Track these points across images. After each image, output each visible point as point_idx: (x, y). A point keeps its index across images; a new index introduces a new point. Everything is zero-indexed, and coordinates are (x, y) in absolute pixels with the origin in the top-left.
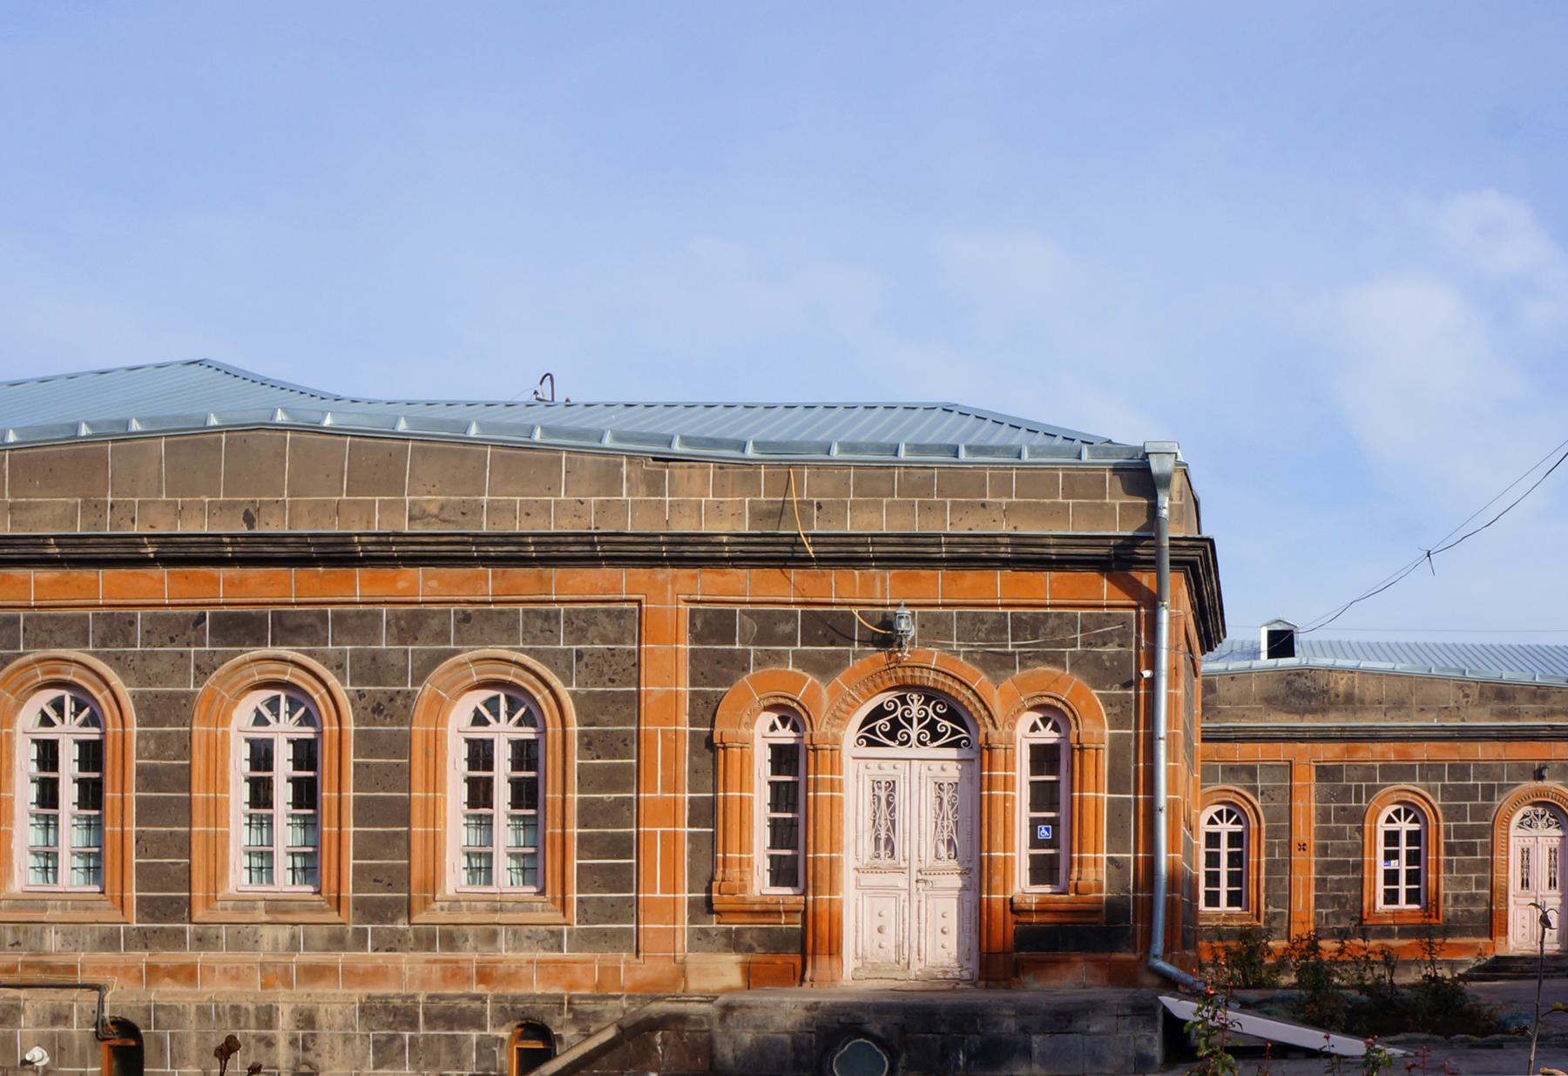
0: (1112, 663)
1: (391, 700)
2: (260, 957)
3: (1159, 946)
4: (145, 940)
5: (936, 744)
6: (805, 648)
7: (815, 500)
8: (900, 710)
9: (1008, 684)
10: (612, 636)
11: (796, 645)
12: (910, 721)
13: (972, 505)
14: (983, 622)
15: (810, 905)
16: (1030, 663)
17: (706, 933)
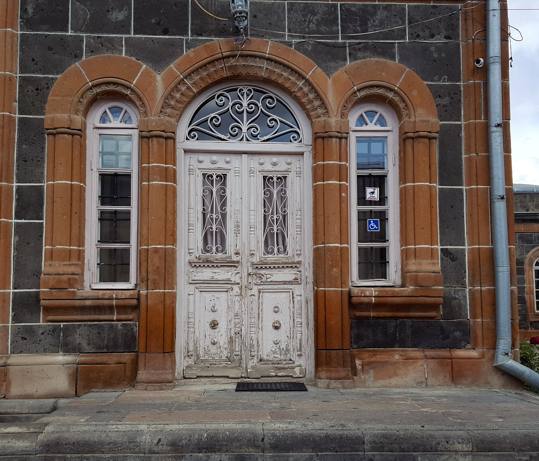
6: (137, 36)
8: (231, 104)
9: (340, 73)
11: (129, 33)
14: (314, 13)
15: (143, 300)
16: (360, 54)
17: (30, 330)
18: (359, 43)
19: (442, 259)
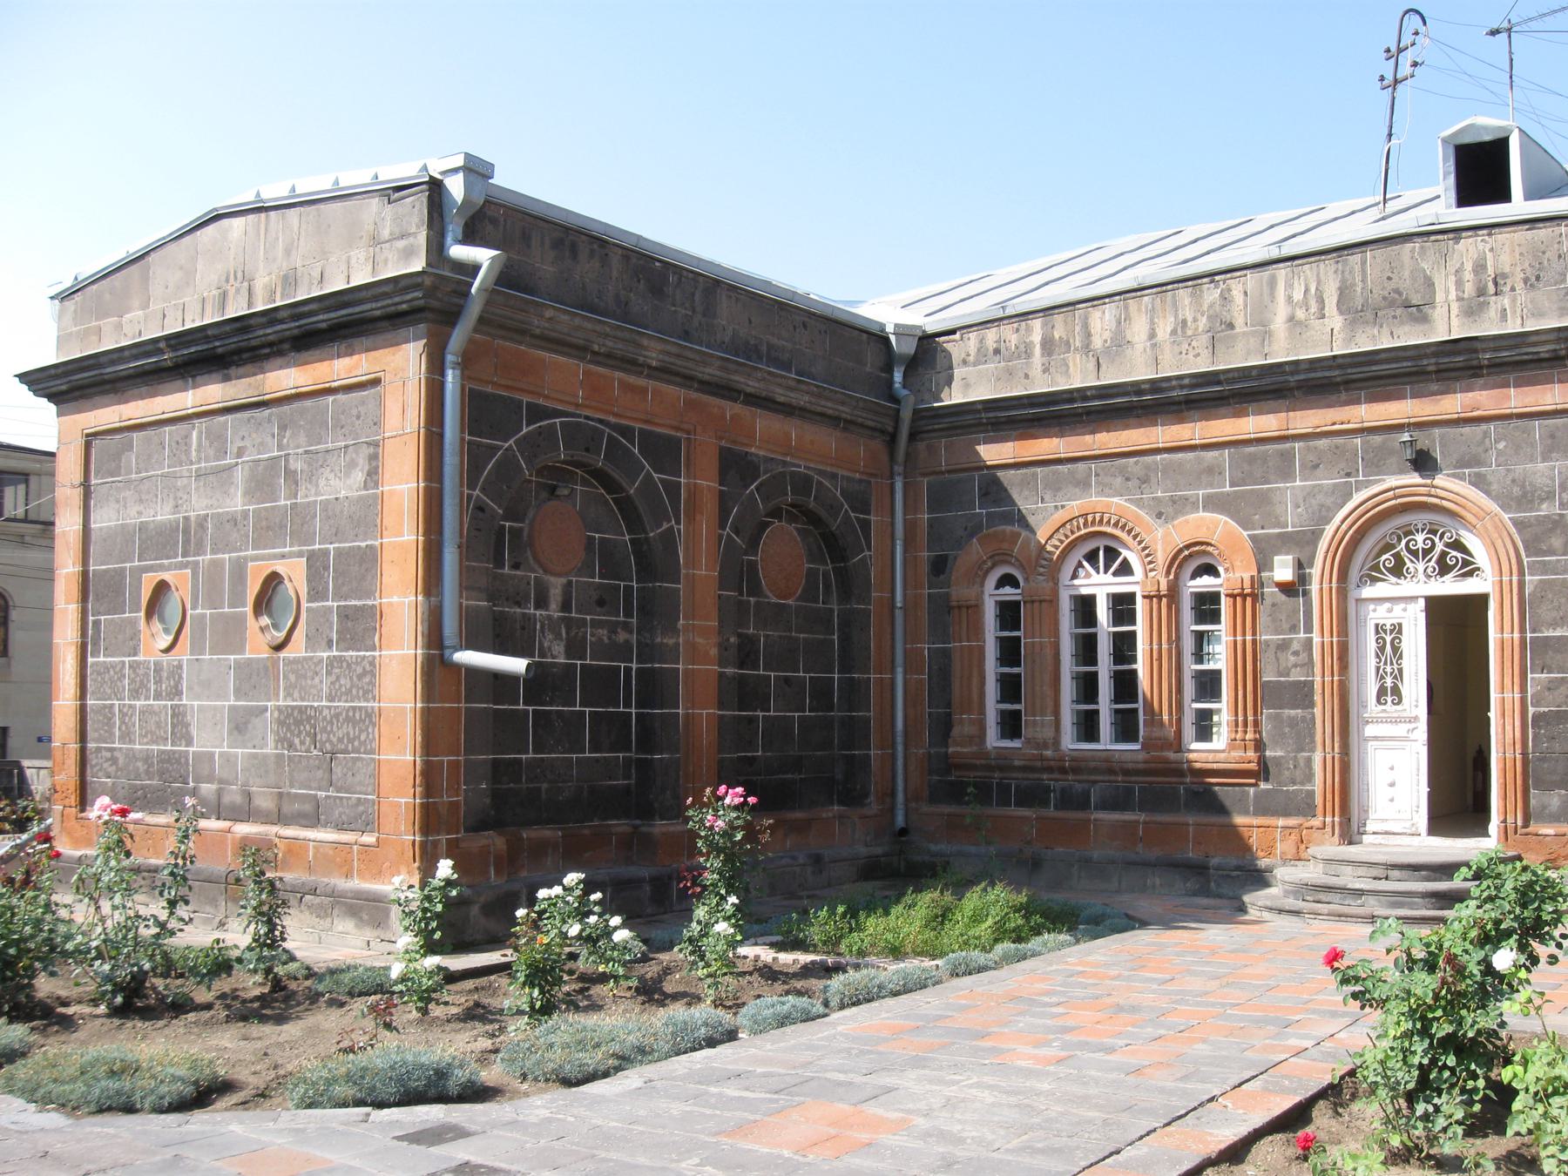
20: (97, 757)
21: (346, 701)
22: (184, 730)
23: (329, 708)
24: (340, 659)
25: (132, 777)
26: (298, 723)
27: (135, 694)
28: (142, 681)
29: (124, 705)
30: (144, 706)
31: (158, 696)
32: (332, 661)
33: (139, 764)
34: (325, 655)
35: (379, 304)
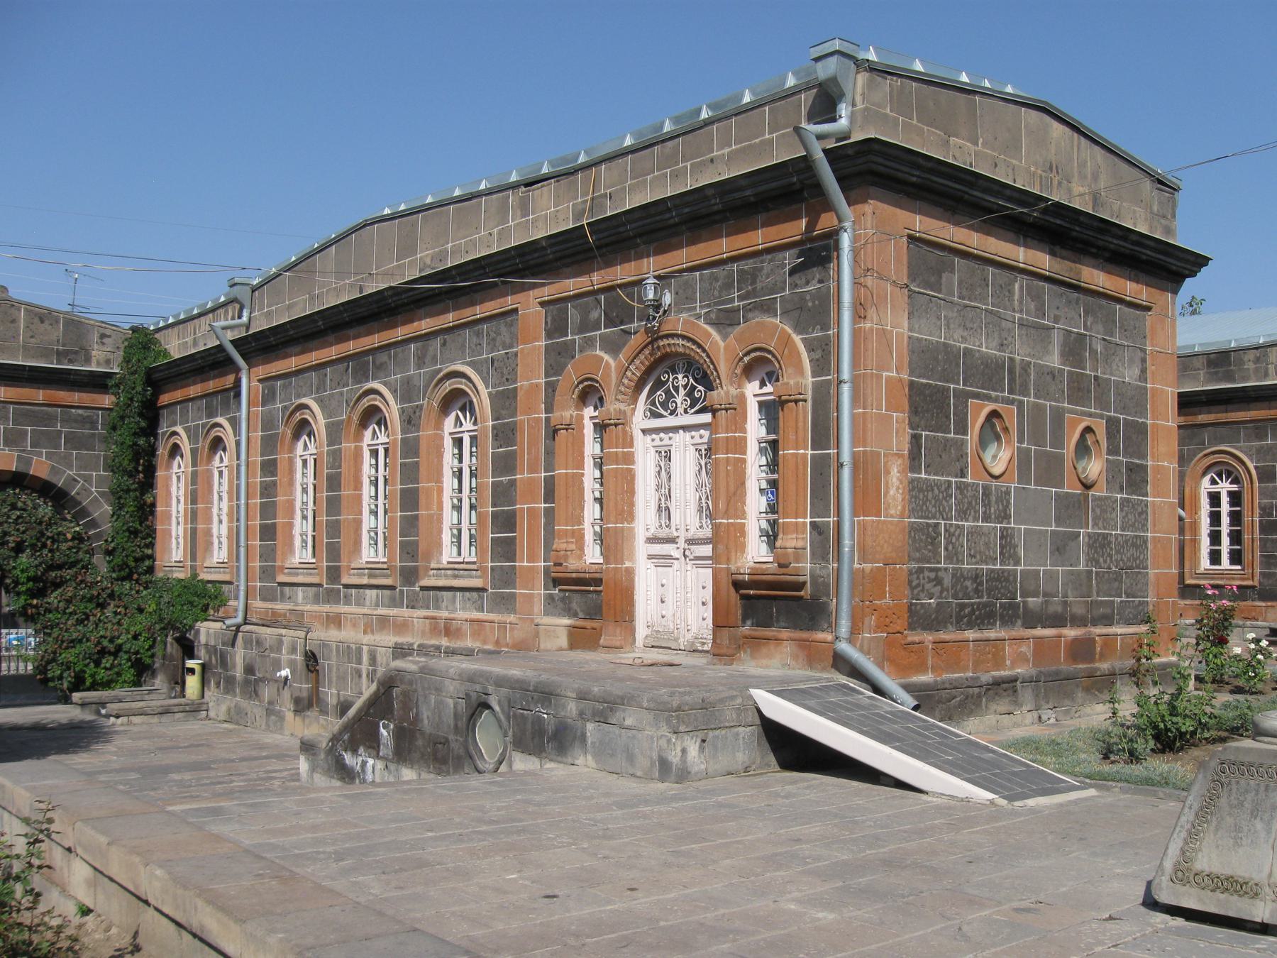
0: (813, 302)
1: (415, 412)
2: (365, 611)
3: (844, 627)
4: (332, 597)
5: (693, 411)
7: (608, 191)
10: (508, 341)
12: (676, 389)
13: (702, 163)
16: (750, 315)
18: (751, 303)
19: (810, 533)
20: (918, 578)
21: (1132, 532)
22: (1012, 551)
23: (1122, 535)
24: (1128, 500)
25: (961, 596)
26: (1102, 547)
27: (963, 515)
28: (970, 503)
29: (951, 525)
30: (972, 527)
31: (986, 518)
32: (1125, 502)
33: (968, 583)
34: (1119, 496)
35: (1179, 264)
